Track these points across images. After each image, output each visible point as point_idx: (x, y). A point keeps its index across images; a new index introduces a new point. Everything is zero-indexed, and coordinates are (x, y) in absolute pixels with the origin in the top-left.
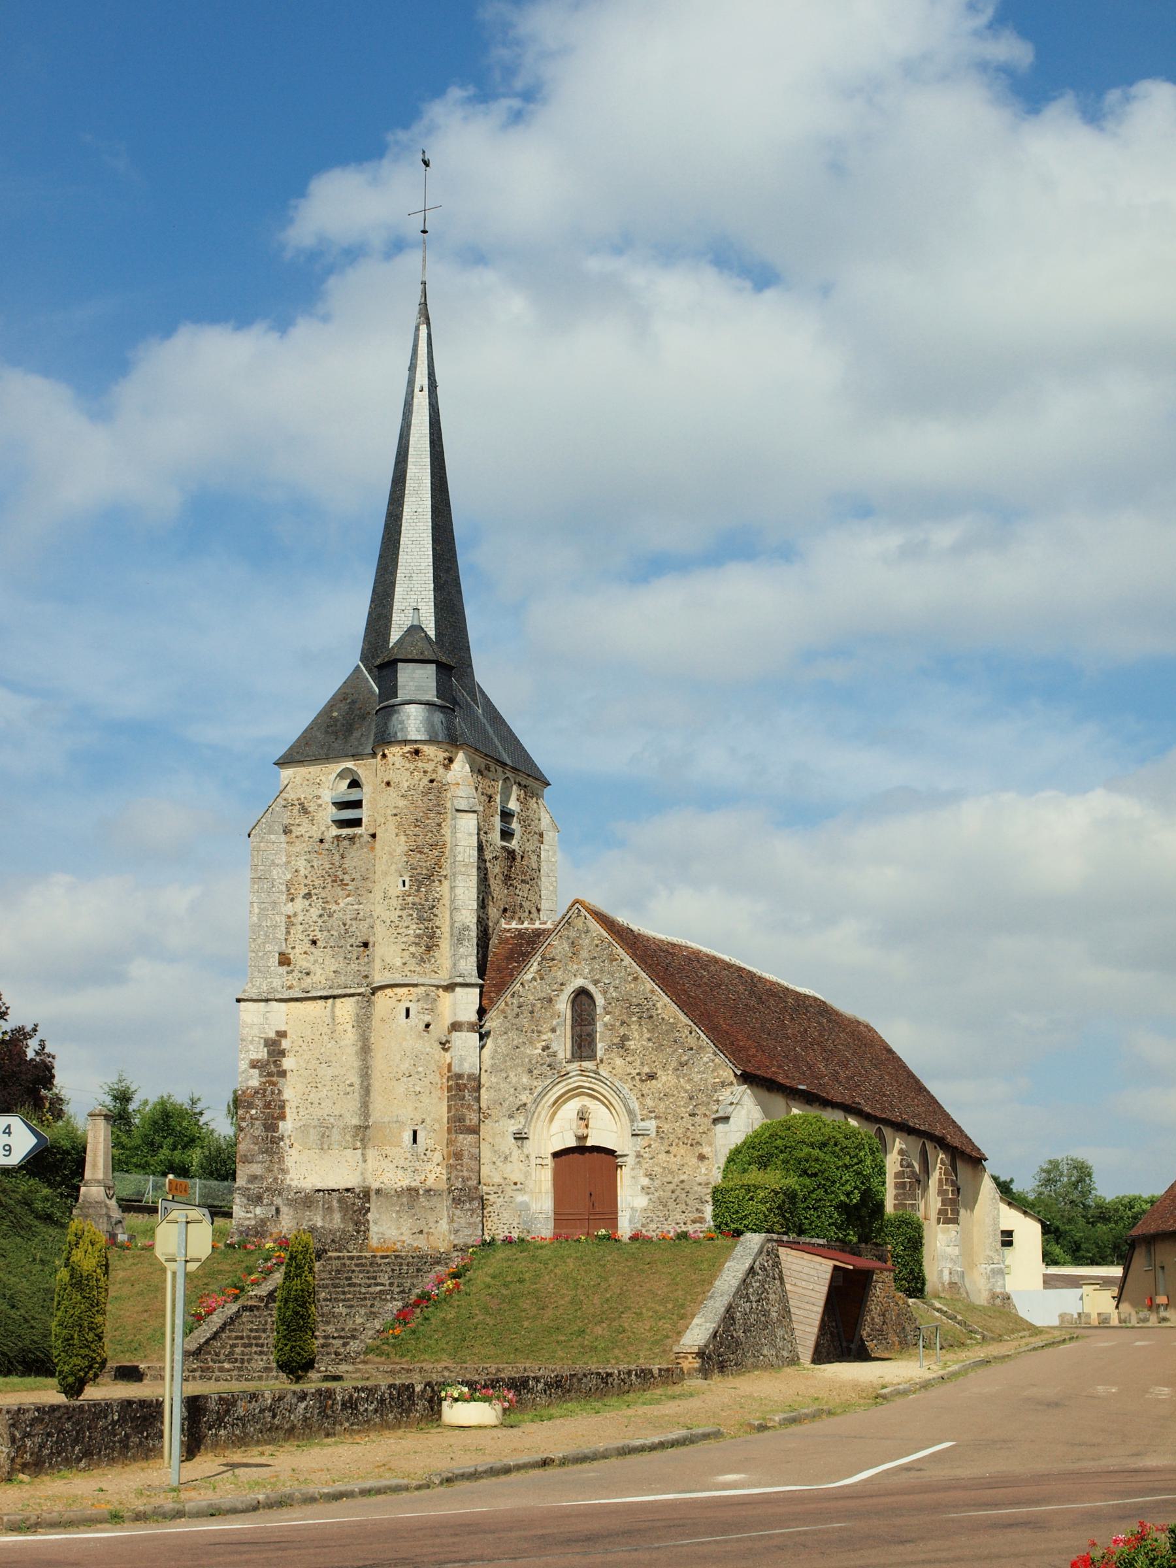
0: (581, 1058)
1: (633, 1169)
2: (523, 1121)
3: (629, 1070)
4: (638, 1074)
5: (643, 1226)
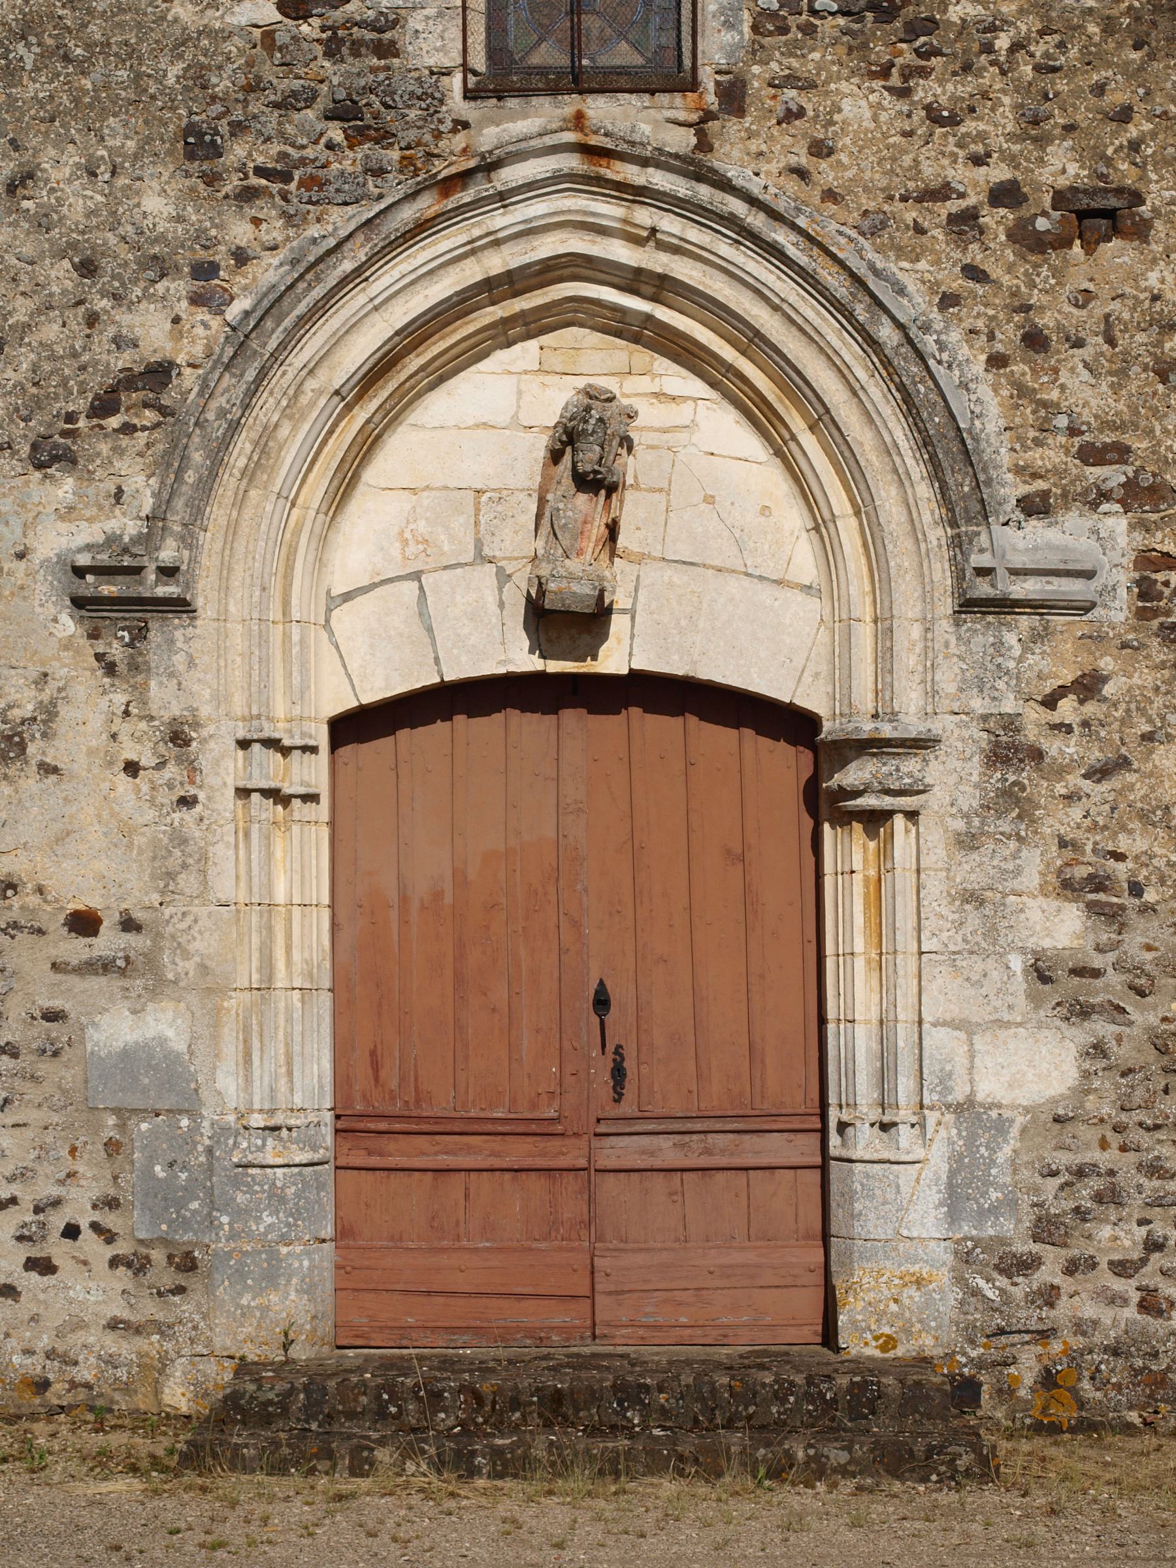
1: (967, 842)
3: (938, 162)
4: (1005, 195)
5: (1046, 1229)
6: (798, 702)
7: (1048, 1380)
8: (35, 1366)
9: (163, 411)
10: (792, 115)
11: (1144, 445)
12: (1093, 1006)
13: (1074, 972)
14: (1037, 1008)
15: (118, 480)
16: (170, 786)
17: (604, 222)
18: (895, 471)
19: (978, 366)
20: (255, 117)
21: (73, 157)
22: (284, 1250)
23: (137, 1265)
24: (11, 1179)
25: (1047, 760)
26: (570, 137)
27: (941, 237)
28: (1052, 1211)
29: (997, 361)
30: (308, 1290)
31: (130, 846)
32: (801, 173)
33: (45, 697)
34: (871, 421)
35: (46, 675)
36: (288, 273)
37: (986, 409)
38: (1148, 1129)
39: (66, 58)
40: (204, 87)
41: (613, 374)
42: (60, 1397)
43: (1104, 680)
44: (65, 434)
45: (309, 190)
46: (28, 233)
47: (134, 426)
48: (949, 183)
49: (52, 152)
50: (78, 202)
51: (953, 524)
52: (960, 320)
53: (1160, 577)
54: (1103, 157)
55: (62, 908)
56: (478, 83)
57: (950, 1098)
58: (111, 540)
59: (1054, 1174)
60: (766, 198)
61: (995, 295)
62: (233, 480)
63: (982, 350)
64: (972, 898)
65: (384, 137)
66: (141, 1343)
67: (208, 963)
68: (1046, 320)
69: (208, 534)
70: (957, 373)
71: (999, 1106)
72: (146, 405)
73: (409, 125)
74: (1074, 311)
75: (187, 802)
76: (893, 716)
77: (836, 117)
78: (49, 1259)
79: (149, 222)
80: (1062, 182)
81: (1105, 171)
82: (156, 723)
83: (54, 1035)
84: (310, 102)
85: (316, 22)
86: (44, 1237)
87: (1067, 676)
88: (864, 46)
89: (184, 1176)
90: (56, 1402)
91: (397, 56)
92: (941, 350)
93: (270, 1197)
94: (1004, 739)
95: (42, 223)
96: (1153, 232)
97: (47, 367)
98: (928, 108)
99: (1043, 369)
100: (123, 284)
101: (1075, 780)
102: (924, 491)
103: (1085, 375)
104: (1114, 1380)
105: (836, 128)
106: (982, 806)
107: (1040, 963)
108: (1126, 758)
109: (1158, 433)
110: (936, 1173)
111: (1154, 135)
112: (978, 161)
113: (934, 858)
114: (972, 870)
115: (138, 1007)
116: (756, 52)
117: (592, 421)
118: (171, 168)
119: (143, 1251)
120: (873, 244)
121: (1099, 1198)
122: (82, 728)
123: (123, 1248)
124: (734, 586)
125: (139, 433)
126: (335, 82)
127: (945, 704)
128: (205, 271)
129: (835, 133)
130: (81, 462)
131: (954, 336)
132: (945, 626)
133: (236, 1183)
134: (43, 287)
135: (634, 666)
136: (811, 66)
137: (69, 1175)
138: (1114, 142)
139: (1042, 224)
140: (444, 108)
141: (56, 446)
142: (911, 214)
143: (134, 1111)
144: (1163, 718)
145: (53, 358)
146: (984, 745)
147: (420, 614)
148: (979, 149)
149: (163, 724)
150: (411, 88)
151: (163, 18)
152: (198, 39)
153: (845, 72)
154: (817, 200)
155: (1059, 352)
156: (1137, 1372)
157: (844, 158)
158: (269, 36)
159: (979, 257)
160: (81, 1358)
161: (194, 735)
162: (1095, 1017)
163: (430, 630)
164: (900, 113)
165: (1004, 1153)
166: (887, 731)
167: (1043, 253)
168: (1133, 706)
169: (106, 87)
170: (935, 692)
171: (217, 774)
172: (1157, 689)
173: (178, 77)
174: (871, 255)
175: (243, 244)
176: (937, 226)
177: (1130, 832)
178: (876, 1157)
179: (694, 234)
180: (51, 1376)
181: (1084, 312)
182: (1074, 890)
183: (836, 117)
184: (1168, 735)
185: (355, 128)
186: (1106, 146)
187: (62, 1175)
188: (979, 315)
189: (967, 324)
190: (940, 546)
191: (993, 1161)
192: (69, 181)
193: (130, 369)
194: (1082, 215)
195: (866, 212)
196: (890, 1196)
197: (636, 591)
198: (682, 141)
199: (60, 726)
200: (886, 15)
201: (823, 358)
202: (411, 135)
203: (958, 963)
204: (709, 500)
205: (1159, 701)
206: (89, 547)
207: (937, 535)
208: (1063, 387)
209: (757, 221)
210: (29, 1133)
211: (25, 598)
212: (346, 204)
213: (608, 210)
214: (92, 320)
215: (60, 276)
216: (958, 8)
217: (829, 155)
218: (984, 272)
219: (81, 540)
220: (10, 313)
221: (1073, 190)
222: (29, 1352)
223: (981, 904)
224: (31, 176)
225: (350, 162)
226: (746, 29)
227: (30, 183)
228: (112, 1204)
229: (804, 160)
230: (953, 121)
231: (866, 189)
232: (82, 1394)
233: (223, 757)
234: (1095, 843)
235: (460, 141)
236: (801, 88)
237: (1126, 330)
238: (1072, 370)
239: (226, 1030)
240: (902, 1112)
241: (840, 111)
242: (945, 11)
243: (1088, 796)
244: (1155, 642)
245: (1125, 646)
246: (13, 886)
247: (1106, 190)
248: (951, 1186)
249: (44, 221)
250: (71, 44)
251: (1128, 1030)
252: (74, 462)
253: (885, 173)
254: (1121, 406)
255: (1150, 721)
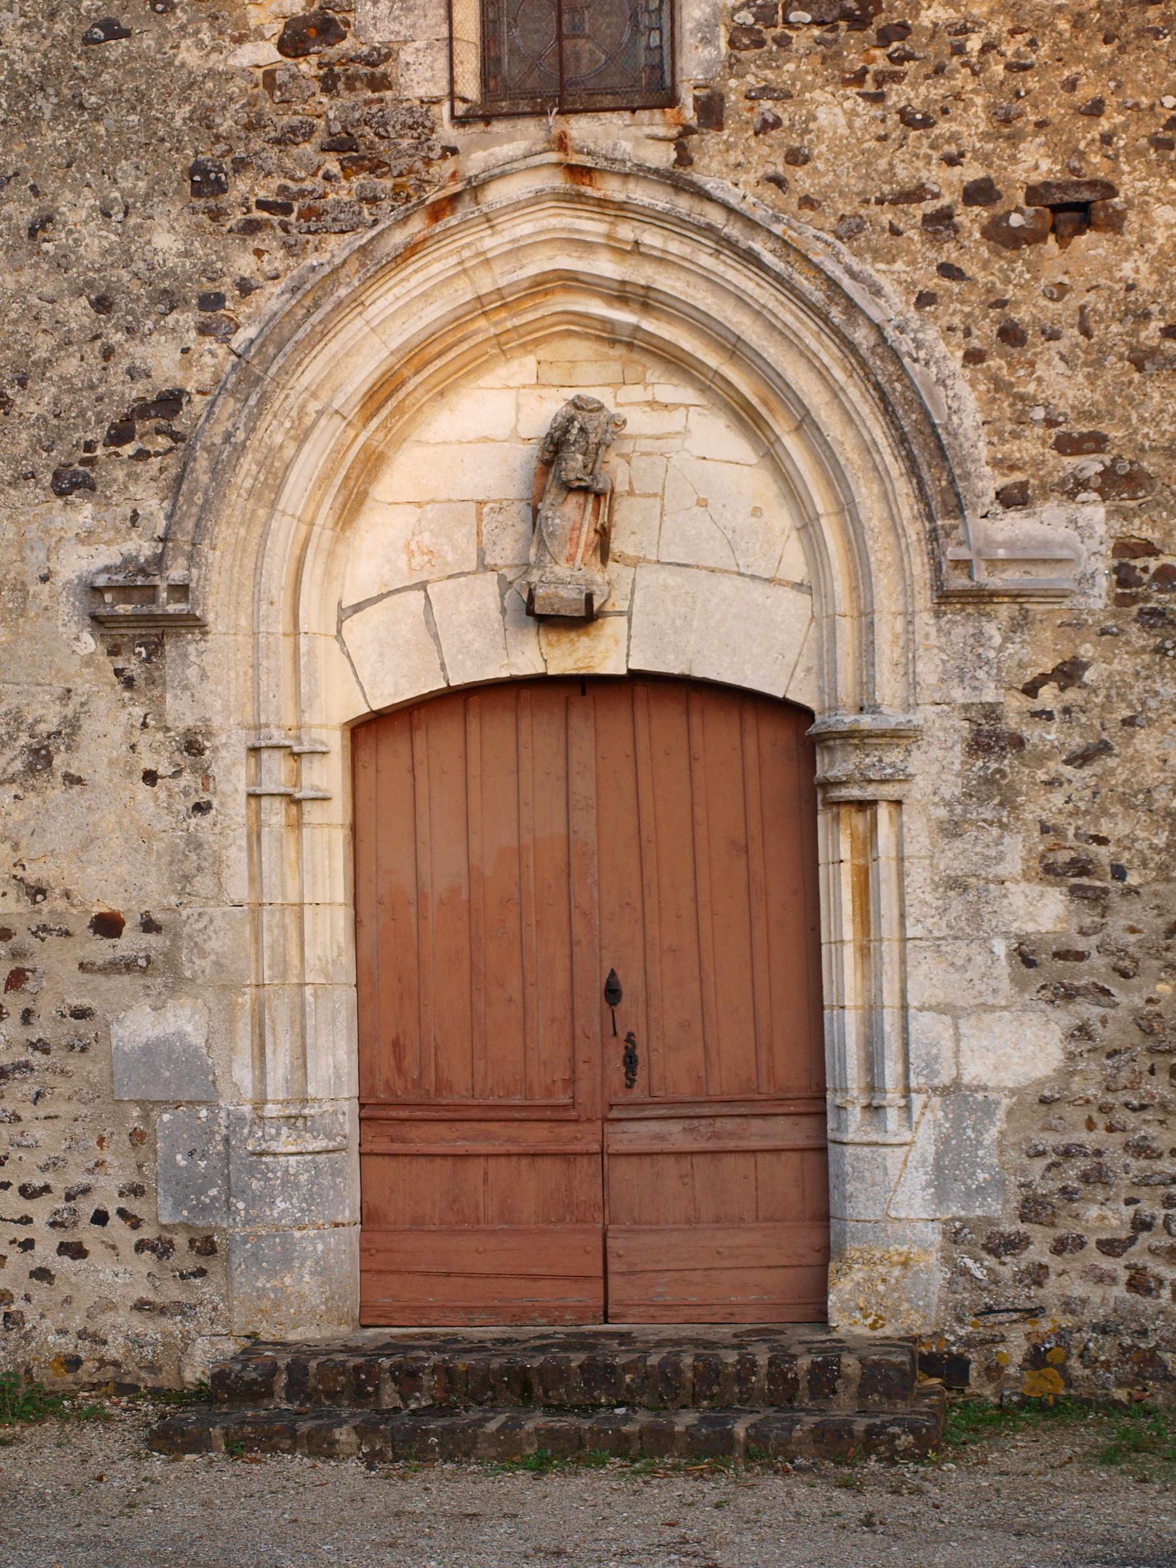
0: (563, 95)
1: (951, 830)
2: (153, 506)
4: (979, 193)
5: (1033, 1208)
6: (790, 696)
7: (1036, 1359)
8: (67, 1344)
9: (176, 437)
10: (768, 126)
11: (1120, 434)
12: (1077, 989)
13: (1058, 955)
14: (1022, 991)
15: (132, 504)
16: (186, 793)
17: (589, 239)
18: (876, 468)
19: (955, 363)
20: (256, 154)
21: (89, 200)
22: (297, 1234)
23: (161, 1249)
24: (44, 1169)
25: (1028, 747)
26: (553, 157)
27: (916, 238)
28: (1039, 1191)
29: (973, 357)
30: (322, 1271)
31: (149, 851)
32: (778, 182)
33: (69, 712)
34: (851, 421)
35: (69, 691)
36: (288, 301)
37: (963, 406)
38: (1134, 1110)
39: (81, 106)
40: (209, 127)
41: (608, 385)
42: (90, 1375)
43: (1085, 666)
44: (83, 462)
45: (308, 220)
46: (48, 273)
47: (148, 452)
48: (923, 185)
49: (69, 196)
50: (93, 242)
51: (930, 518)
52: (937, 318)
53: (1139, 563)
54: (1075, 150)
55: (87, 912)
56: (468, 110)
57: (936, 1082)
58: (128, 560)
59: (1041, 1154)
60: (743, 207)
61: (971, 292)
62: (240, 500)
63: (959, 346)
64: (956, 884)
65: (376, 167)
66: (167, 1323)
67: (223, 961)
68: (1022, 315)
69: (218, 553)
70: (934, 369)
71: (985, 1089)
72: (158, 432)
73: (400, 154)
74: (1051, 305)
75: (201, 808)
76: (875, 709)
77: (812, 126)
78: (80, 1244)
79: (159, 258)
80: (1036, 178)
81: (1076, 164)
82: (172, 734)
83: (81, 1032)
84: (308, 136)
85: (314, 59)
86: (75, 1223)
87: (1048, 664)
88: (838, 54)
89: (203, 1164)
90: (86, 1379)
91: (389, 88)
92: (918, 348)
93: (283, 1184)
94: (986, 727)
95: (61, 264)
96: (1126, 223)
97: (67, 400)
98: (902, 112)
99: (1019, 362)
100: (136, 319)
101: (1056, 767)
102: (903, 488)
103: (1061, 367)
104: (1102, 1358)
105: (812, 136)
106: (964, 794)
107: (1024, 947)
108: (1106, 743)
109: (1134, 421)
110: (922, 1155)
111: (1125, 127)
112: (952, 161)
113: (918, 846)
114: (955, 858)
115: (159, 1004)
116: (733, 66)
117: (575, 431)
118: (179, 205)
119: (168, 1236)
120: (850, 247)
121: (1085, 1178)
122: (103, 741)
123: (148, 1233)
124: (727, 585)
125: (153, 459)
126: (331, 115)
127: (925, 695)
128: (210, 302)
129: (811, 141)
130: (99, 488)
131: (931, 334)
132: (925, 620)
133: (251, 1170)
134: (63, 324)
135: (631, 667)
136: (786, 77)
137: (97, 1165)
138: (1088, 135)
139: (1016, 220)
140: (434, 136)
141: (76, 473)
142: (887, 216)
143: (156, 1103)
144: (1143, 704)
145: (72, 390)
146: (965, 734)
147: (427, 622)
148: (953, 149)
149: (178, 734)
150: (402, 118)
151: (171, 64)
152: (203, 82)
153: (819, 81)
154: (794, 207)
155: (1034, 345)
156: (1124, 1350)
157: (820, 165)
158: (269, 75)
159: (954, 255)
160: (110, 1338)
161: (207, 744)
162: (1079, 999)
163: (436, 637)
164: (874, 118)
165: (991, 1135)
166: (866, 722)
167: (1017, 248)
168: (1113, 692)
169: (119, 133)
170: (916, 684)
171: (229, 781)
172: (1137, 674)
173: (184, 119)
174: (849, 259)
175: (247, 275)
176: (913, 227)
177: (1113, 816)
178: (866, 1139)
179: (675, 247)
180: (82, 1355)
181: (1059, 305)
182: (1057, 875)
183: (812, 126)
184: (1149, 719)
185: (350, 159)
186: (1078, 141)
187: (91, 1164)
188: (954, 313)
189: (945, 321)
190: (919, 540)
191: (979, 1144)
192: (85, 223)
193: (144, 399)
194: (1056, 209)
195: (843, 217)
196: (879, 1179)
197: (632, 593)
198: (662, 156)
199: (83, 738)
200: (859, 22)
201: (804, 361)
202: (402, 164)
203: (943, 948)
204: (702, 503)
205: (1139, 686)
206: (107, 569)
207: (914, 530)
208: (1039, 380)
209: (734, 230)
210: (59, 1125)
211: (49, 619)
212: (342, 232)
213: (592, 226)
214: (108, 353)
215: (78, 311)
216: (930, 12)
217: (805, 162)
218: (959, 270)
219: (100, 563)
220: (32, 350)
221: (1047, 185)
222: (62, 1332)
223: (965, 890)
224: (50, 219)
225: (344, 192)
226: (723, 43)
227: (49, 226)
228: (137, 1191)
229: (780, 168)
230: (927, 123)
231: (842, 194)
232: (110, 1372)
233: (234, 764)
234: (1078, 828)
235: (449, 166)
236: (777, 99)
237: (1102, 320)
238: (1048, 363)
239: (240, 1025)
240: (889, 1096)
241: (815, 119)
242: (918, 15)
243: (1070, 781)
244: (1134, 628)
245: (1104, 632)
246: (42, 891)
247: (1078, 184)
248: (938, 1167)
249: (63, 261)
250: (85, 94)
251: (1112, 1012)
252: (93, 488)
253: (860, 178)
254: (1097, 396)
255: (1130, 706)
